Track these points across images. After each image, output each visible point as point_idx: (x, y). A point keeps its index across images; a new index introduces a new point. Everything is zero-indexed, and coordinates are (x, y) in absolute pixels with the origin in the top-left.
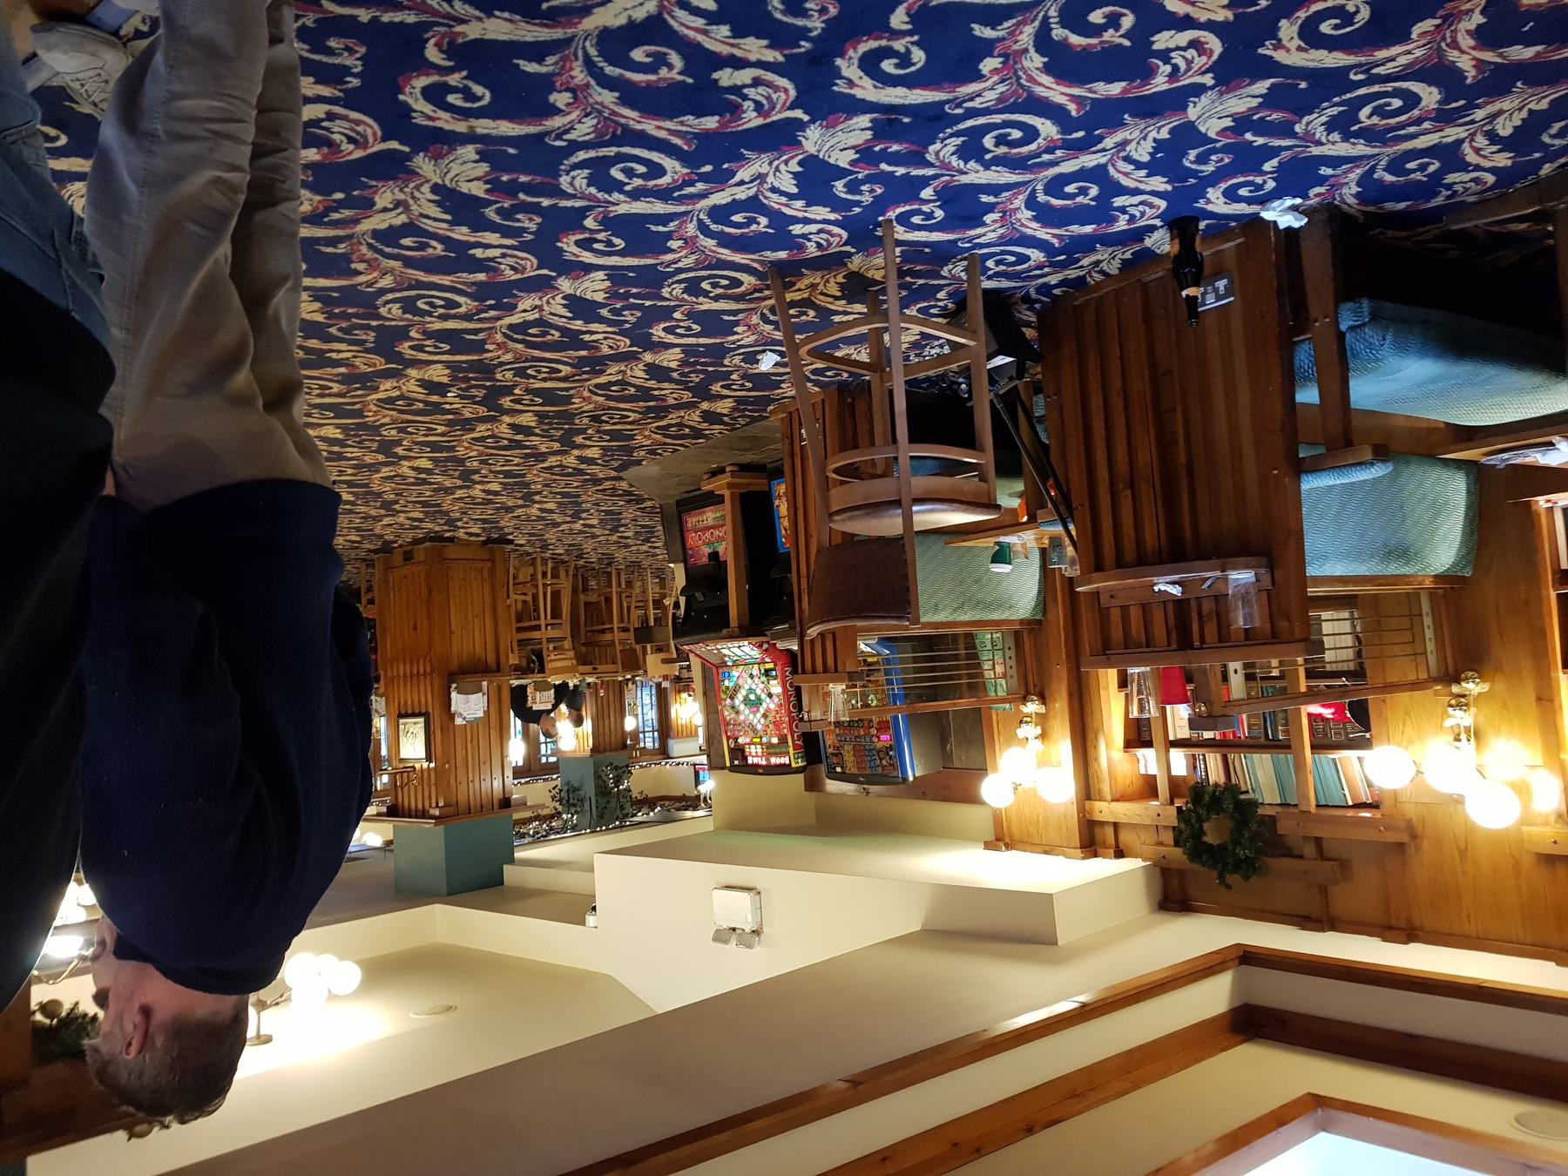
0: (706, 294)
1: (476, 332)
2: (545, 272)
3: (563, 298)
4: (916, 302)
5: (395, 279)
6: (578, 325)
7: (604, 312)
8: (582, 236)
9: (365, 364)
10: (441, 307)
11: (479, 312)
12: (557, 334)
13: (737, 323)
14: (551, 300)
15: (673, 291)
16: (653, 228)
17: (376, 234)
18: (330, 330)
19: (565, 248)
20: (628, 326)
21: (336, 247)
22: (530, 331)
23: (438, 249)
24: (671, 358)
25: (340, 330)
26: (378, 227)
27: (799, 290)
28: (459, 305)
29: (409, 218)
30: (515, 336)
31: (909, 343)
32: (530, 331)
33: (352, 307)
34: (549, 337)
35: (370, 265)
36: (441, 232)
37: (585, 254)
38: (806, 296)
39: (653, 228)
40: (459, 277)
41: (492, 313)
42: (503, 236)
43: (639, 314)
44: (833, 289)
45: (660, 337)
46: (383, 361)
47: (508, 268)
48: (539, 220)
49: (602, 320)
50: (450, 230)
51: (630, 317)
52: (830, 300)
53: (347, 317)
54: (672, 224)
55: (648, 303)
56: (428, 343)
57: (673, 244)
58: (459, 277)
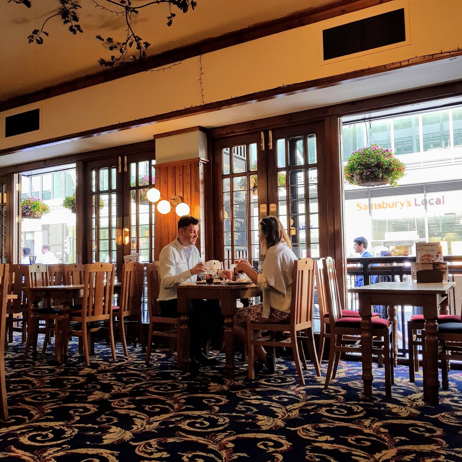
0: (206, 419)
1: (313, 399)
2: (292, 429)
3: (278, 416)
4: (91, 414)
5: (363, 424)
6: (266, 403)
7: (255, 410)
8: (281, 449)
9: (356, 384)
10: (335, 410)
11: (316, 408)
12: (274, 398)
13: (185, 404)
14: (284, 415)
15: (224, 420)
16: (245, 455)
17: (386, 448)
18: (380, 399)
19: (286, 442)
20: (240, 403)
21: (401, 439)
22: (288, 400)
23: (351, 439)
24: (214, 386)
25: (377, 400)
26: (386, 451)
27: (156, 421)
28: (327, 411)
29: (374, 457)
30: (293, 397)
31: (93, 394)
32: (288, 400)
33: (375, 410)
34: (277, 397)
35: (380, 431)
36: (353, 449)
37: (276, 439)
38: (152, 418)
39: (245, 455)
40: (333, 425)
41: (309, 408)
42: (321, 447)
43: (237, 408)
44: (138, 421)
45: (223, 397)
46: (349, 385)
47: (311, 430)
48: (307, 458)
49: (254, 405)
50: (349, 450)
51: (240, 407)
52: (138, 416)
53: (376, 405)
54: (236, 457)
55: (234, 414)
56: (334, 394)
57: (231, 445)
58: (333, 425)
